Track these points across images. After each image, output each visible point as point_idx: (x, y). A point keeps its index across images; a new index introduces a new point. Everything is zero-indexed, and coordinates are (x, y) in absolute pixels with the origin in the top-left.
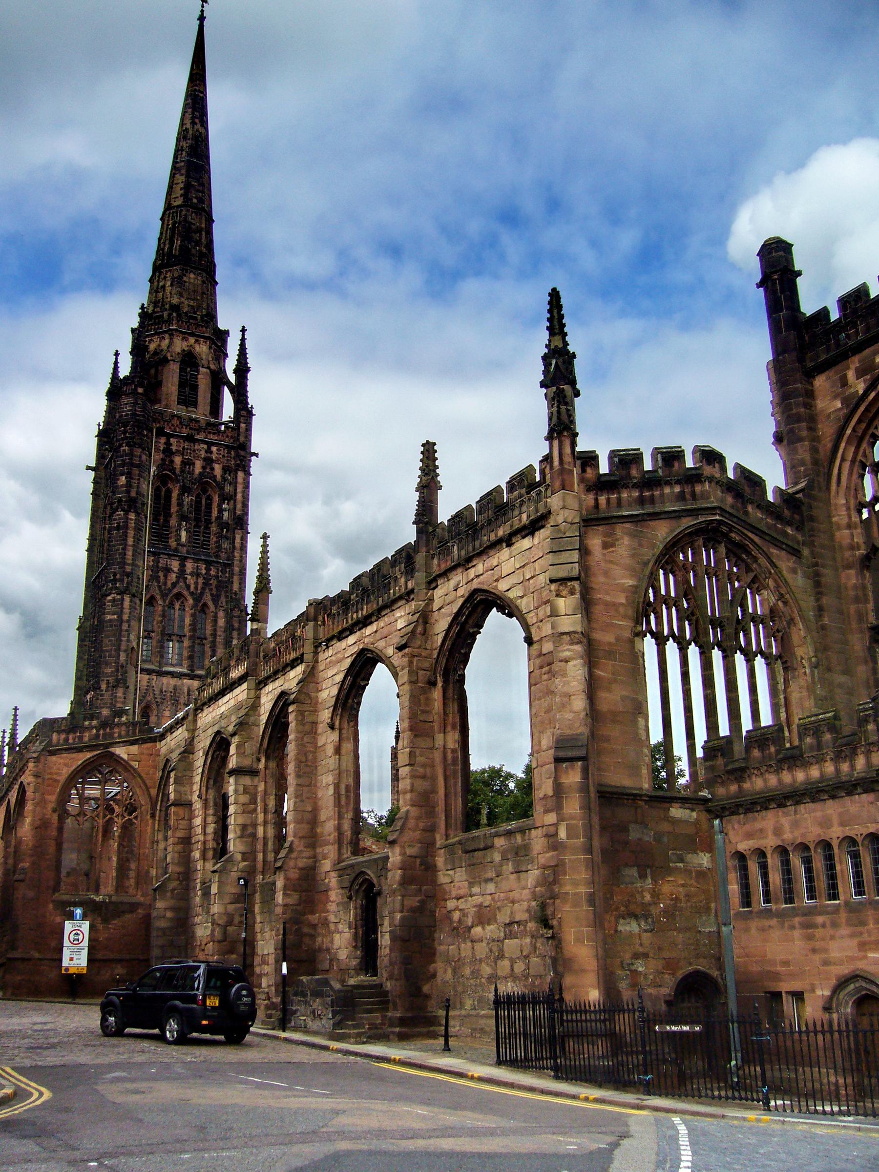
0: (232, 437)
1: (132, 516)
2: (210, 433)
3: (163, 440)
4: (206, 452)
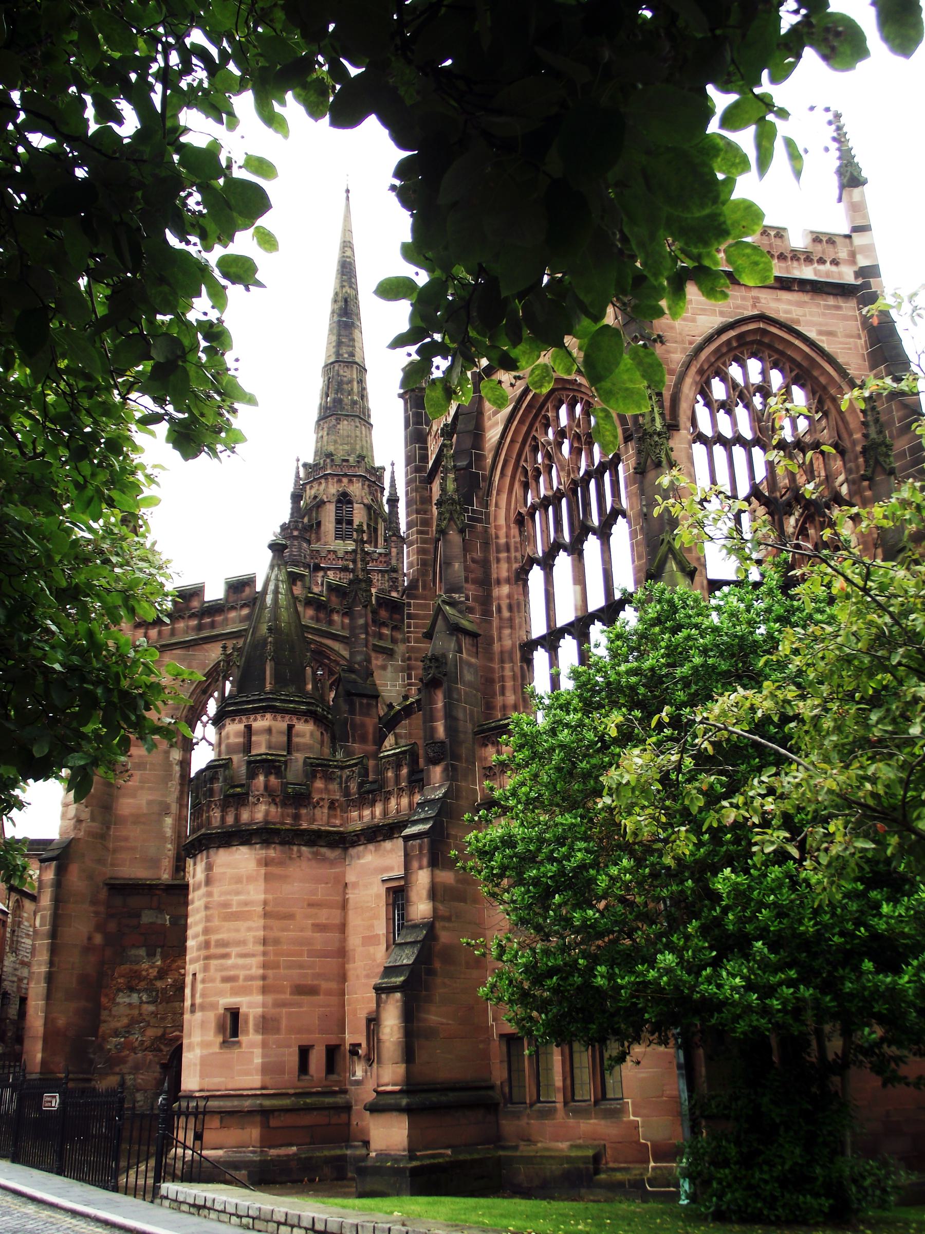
3: (321, 574)
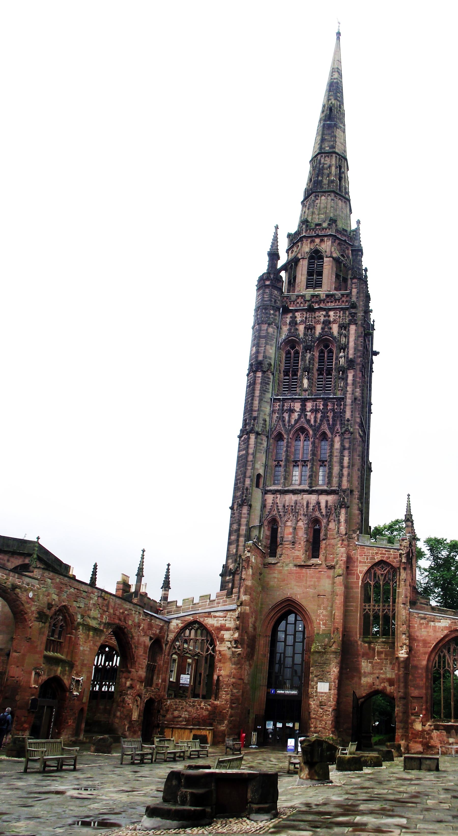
0: (347, 301)
1: (259, 374)
2: (328, 302)
3: (290, 315)
4: (325, 316)
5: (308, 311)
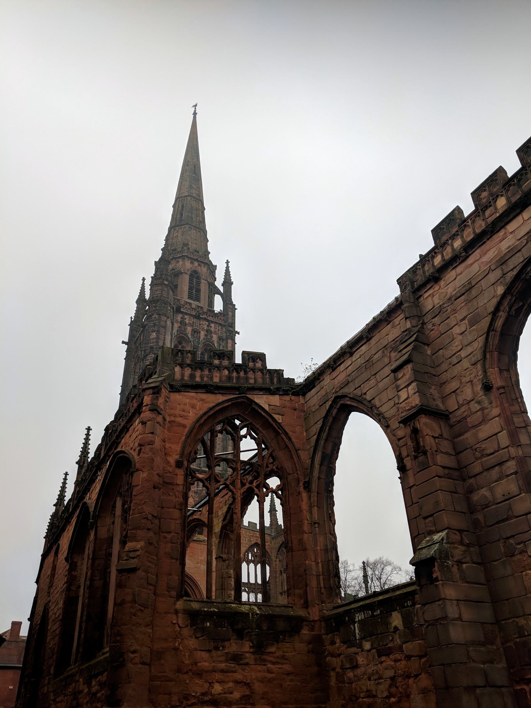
2: (210, 316)
4: (208, 326)
5: (195, 318)
